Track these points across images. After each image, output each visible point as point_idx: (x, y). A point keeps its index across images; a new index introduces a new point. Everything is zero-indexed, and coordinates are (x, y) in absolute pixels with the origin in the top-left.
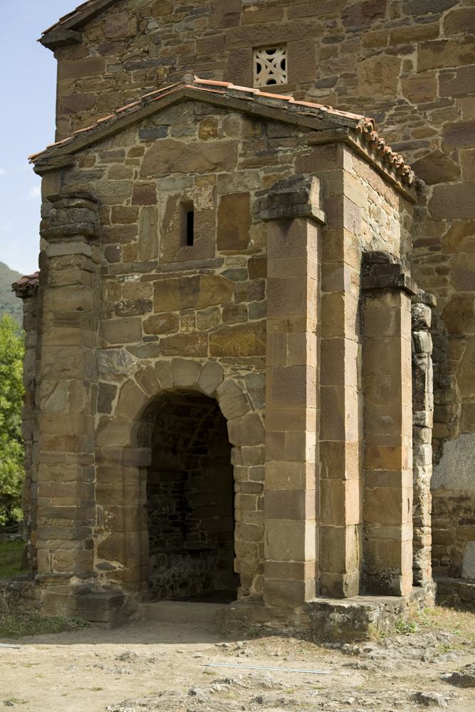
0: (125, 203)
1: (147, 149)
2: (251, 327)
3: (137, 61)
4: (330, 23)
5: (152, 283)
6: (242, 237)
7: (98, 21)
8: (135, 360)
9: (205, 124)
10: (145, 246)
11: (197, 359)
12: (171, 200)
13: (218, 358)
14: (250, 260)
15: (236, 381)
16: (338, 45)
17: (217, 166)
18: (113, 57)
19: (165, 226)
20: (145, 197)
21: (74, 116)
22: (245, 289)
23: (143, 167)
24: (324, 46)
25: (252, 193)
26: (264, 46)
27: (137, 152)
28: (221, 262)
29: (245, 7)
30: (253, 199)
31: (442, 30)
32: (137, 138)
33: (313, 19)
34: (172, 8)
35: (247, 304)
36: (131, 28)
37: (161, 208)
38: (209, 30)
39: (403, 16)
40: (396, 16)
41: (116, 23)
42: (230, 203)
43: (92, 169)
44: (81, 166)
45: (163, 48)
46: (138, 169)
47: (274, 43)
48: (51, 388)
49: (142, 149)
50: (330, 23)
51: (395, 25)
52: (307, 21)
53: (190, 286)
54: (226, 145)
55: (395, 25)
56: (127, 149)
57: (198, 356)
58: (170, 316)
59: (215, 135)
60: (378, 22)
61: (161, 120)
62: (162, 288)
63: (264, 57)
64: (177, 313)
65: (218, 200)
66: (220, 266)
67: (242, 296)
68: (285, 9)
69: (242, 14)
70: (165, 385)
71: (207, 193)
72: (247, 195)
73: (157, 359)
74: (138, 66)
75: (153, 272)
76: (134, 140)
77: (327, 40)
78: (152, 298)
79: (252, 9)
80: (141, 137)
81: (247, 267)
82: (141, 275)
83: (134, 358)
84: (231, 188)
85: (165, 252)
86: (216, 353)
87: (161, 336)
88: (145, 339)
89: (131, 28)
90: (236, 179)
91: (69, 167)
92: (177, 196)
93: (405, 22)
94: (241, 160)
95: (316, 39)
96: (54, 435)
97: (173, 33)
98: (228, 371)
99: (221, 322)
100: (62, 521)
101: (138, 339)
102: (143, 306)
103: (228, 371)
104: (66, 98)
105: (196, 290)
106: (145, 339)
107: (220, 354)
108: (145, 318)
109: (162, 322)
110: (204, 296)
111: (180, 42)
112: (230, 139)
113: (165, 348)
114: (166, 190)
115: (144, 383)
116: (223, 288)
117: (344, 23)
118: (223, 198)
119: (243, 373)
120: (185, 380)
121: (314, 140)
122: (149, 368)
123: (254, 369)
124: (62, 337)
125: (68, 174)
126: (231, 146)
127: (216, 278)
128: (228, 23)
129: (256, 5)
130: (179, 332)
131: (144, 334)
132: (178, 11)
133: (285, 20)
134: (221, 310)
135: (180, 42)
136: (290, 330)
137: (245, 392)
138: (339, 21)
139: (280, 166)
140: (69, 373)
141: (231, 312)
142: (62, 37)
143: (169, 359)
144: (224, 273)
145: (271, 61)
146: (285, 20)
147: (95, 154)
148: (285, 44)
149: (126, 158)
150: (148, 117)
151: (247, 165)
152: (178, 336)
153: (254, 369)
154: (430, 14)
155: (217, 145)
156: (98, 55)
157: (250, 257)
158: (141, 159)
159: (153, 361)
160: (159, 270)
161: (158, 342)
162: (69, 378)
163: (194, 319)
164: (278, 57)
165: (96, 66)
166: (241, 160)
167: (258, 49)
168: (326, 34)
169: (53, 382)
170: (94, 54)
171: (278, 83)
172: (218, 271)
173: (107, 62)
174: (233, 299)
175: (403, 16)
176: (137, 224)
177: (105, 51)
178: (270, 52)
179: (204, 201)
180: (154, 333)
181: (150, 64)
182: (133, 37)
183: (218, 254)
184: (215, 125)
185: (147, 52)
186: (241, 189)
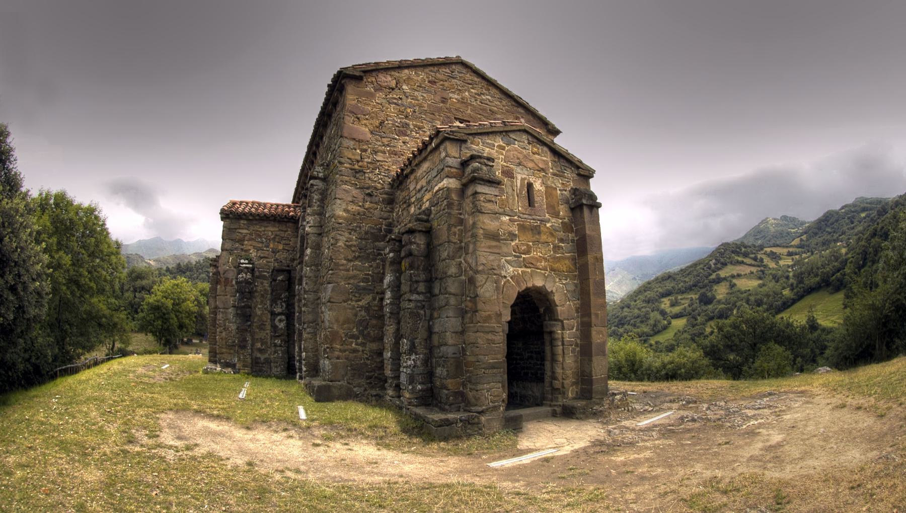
7: (374, 74)
8: (511, 269)
10: (511, 201)
12: (523, 180)
20: (509, 174)
28: (548, 221)
36: (394, 86)
44: (472, 143)
53: (536, 230)
56: (496, 144)
58: (528, 245)
59: (539, 154)
61: (512, 135)
62: (522, 228)
67: (562, 240)
70: (530, 285)
74: (395, 104)
76: (499, 141)
86: (552, 269)
88: (515, 256)
89: (394, 86)
91: (465, 141)
92: (525, 179)
96: (488, 313)
100: (495, 371)
101: (511, 255)
102: (513, 236)
105: (539, 233)
106: (515, 256)
107: (554, 271)
108: (513, 244)
110: (544, 237)
113: (526, 264)
114: (520, 176)
115: (518, 283)
116: (552, 235)
120: (539, 283)
124: (489, 247)
125: (463, 146)
126: (546, 162)
128: (443, 102)
133: (469, 111)
141: (556, 248)
142: (357, 74)
143: (529, 270)
147: (478, 139)
150: (506, 132)
152: (532, 257)
159: (520, 270)
160: (519, 217)
165: (371, 96)
169: (485, 277)
170: (370, 88)
172: (548, 225)
177: (376, 90)
179: (538, 186)
182: (393, 89)
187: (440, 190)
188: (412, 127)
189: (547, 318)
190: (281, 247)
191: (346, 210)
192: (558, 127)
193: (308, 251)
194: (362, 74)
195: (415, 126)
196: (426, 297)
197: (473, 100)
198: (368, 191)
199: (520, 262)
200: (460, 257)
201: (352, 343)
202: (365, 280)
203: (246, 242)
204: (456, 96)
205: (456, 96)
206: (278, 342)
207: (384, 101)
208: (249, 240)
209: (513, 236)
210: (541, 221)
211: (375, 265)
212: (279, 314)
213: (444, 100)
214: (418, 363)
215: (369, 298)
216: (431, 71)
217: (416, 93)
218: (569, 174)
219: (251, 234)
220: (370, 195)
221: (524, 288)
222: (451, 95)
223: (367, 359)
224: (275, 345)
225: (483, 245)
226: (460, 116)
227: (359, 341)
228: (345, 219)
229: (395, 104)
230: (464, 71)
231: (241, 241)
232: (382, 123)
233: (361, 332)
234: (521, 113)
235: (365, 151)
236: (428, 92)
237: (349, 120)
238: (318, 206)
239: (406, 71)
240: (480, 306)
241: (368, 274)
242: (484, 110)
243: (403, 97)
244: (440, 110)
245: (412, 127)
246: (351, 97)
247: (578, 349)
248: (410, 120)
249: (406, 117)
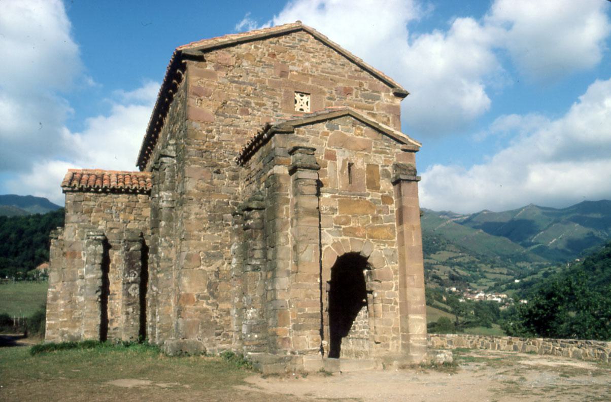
0: (321, 157)
1: (330, 134)
2: (386, 227)
3: (236, 79)
4: (330, 91)
5: (337, 199)
6: (377, 185)
7: (214, 52)
9: (358, 128)
11: (362, 239)
12: (344, 161)
13: (371, 240)
14: (382, 196)
15: (379, 251)
16: (334, 103)
17: (364, 150)
18: (222, 73)
19: (342, 171)
20: (331, 156)
21: (199, 98)
22: (381, 209)
23: (330, 142)
24: (327, 100)
25: (380, 165)
26: (299, 92)
27: (327, 134)
28: (369, 194)
29: (291, 71)
30: (380, 168)
31: (375, 109)
32: (325, 127)
33: (323, 87)
34: (255, 59)
35: (382, 215)
36: (233, 61)
37: (339, 163)
38: (274, 76)
39: (360, 98)
40: (357, 97)
41: (223, 56)
42: (371, 168)
43: (303, 136)
45: (250, 78)
46: (327, 142)
47: (305, 92)
48: (304, 248)
49: (328, 133)
50: (330, 91)
51: (356, 100)
52: (320, 87)
54: (367, 141)
55: (356, 100)
57: (362, 238)
58: (346, 217)
59: (362, 135)
60: (349, 97)
63: (298, 96)
64: (350, 216)
65: (365, 166)
66: (368, 196)
67: (379, 212)
68: (310, 78)
69: (289, 74)
71: (360, 161)
72: (378, 166)
73: (341, 238)
74: (236, 82)
75: (337, 194)
76: (323, 127)
77: (330, 99)
78: (337, 207)
79: (295, 73)
80: (327, 126)
81: (380, 199)
82: (331, 195)
83: (330, 236)
84: (371, 161)
85: (342, 185)
86: (371, 237)
87: (343, 226)
88: (335, 227)
90: (372, 157)
91: (293, 132)
93: (361, 101)
94: (373, 149)
95: (323, 96)
97: (256, 71)
98: (375, 246)
99: (371, 222)
103: (375, 246)
104: (194, 87)
106: (335, 227)
107: (372, 237)
108: (335, 216)
109: (343, 220)
111: (259, 77)
112: (368, 138)
113: (346, 232)
115: (337, 249)
116: (371, 206)
117: (336, 93)
118: (368, 165)
119: (382, 248)
120: (357, 250)
121: (405, 148)
122: (338, 241)
123: (387, 246)
124: (309, 222)
127: (367, 202)
128: (281, 76)
129: (297, 71)
130: (351, 225)
131: (334, 225)
132: (258, 61)
134: (371, 217)
135: (259, 77)
136: (414, 230)
137: (384, 256)
138: (334, 92)
139: (389, 156)
140: (313, 241)
141: (375, 219)
143: (348, 238)
144: (371, 200)
145: (302, 100)
146: (310, 83)
147: (302, 128)
148: (309, 94)
149: (320, 135)
151: (376, 152)
152: (352, 227)
153: (387, 246)
154: (370, 101)
155: (363, 140)
156: (213, 69)
157: (381, 194)
158: (328, 137)
159: (340, 238)
160: (339, 194)
161: (342, 229)
162: (314, 243)
163: (358, 219)
164: (305, 98)
166: (373, 149)
167: (297, 92)
168: (328, 95)
170: (210, 67)
171: (305, 111)
172: (368, 198)
173: (218, 75)
174: (376, 213)
175: (360, 98)
176: (327, 169)
178: (302, 96)
179: (360, 164)
180: (340, 224)
181: (244, 83)
183: (367, 191)
184: (362, 130)
185: (241, 76)
186: (375, 163)
187: (271, 175)
188: (253, 105)
189: (369, 280)
190: (132, 217)
191: (197, 188)
192: (404, 88)
193: (163, 223)
194: (200, 53)
195: (257, 104)
196: (262, 262)
197: (314, 70)
198: (215, 169)
199: (340, 231)
200: (287, 230)
201: (203, 302)
202: (215, 248)
203: (94, 214)
204: (296, 68)
205: (296, 68)
206: (130, 310)
207: (226, 81)
208: (98, 211)
209: (333, 210)
210: (361, 195)
211: (223, 235)
212: (133, 282)
213: (284, 74)
214: (255, 315)
215: (219, 262)
216: (271, 43)
217: (257, 69)
218: (398, 149)
219: (100, 205)
220: (218, 172)
221: (342, 254)
222: (291, 67)
223: (217, 317)
224: (127, 313)
225: (303, 220)
226: (298, 91)
227: (210, 301)
228: (195, 195)
229: (236, 82)
230: (306, 36)
231: (89, 212)
232: (225, 103)
233: (212, 294)
234: (364, 78)
235: (211, 131)
236: (269, 66)
237: (193, 102)
238: (170, 182)
239: (244, 45)
240: (301, 268)
241: (217, 243)
242: (326, 79)
243: (244, 74)
244: (279, 85)
245: (253, 105)
246: (193, 75)
247: (398, 307)
248: (251, 97)
249: (248, 95)
